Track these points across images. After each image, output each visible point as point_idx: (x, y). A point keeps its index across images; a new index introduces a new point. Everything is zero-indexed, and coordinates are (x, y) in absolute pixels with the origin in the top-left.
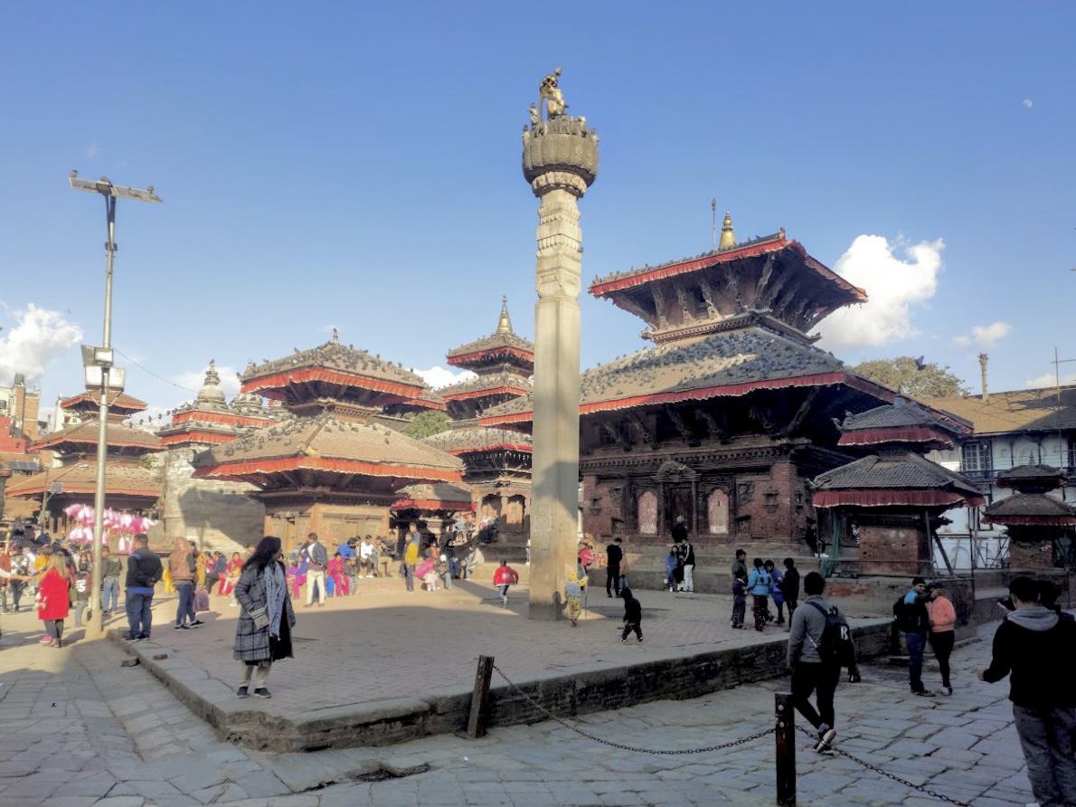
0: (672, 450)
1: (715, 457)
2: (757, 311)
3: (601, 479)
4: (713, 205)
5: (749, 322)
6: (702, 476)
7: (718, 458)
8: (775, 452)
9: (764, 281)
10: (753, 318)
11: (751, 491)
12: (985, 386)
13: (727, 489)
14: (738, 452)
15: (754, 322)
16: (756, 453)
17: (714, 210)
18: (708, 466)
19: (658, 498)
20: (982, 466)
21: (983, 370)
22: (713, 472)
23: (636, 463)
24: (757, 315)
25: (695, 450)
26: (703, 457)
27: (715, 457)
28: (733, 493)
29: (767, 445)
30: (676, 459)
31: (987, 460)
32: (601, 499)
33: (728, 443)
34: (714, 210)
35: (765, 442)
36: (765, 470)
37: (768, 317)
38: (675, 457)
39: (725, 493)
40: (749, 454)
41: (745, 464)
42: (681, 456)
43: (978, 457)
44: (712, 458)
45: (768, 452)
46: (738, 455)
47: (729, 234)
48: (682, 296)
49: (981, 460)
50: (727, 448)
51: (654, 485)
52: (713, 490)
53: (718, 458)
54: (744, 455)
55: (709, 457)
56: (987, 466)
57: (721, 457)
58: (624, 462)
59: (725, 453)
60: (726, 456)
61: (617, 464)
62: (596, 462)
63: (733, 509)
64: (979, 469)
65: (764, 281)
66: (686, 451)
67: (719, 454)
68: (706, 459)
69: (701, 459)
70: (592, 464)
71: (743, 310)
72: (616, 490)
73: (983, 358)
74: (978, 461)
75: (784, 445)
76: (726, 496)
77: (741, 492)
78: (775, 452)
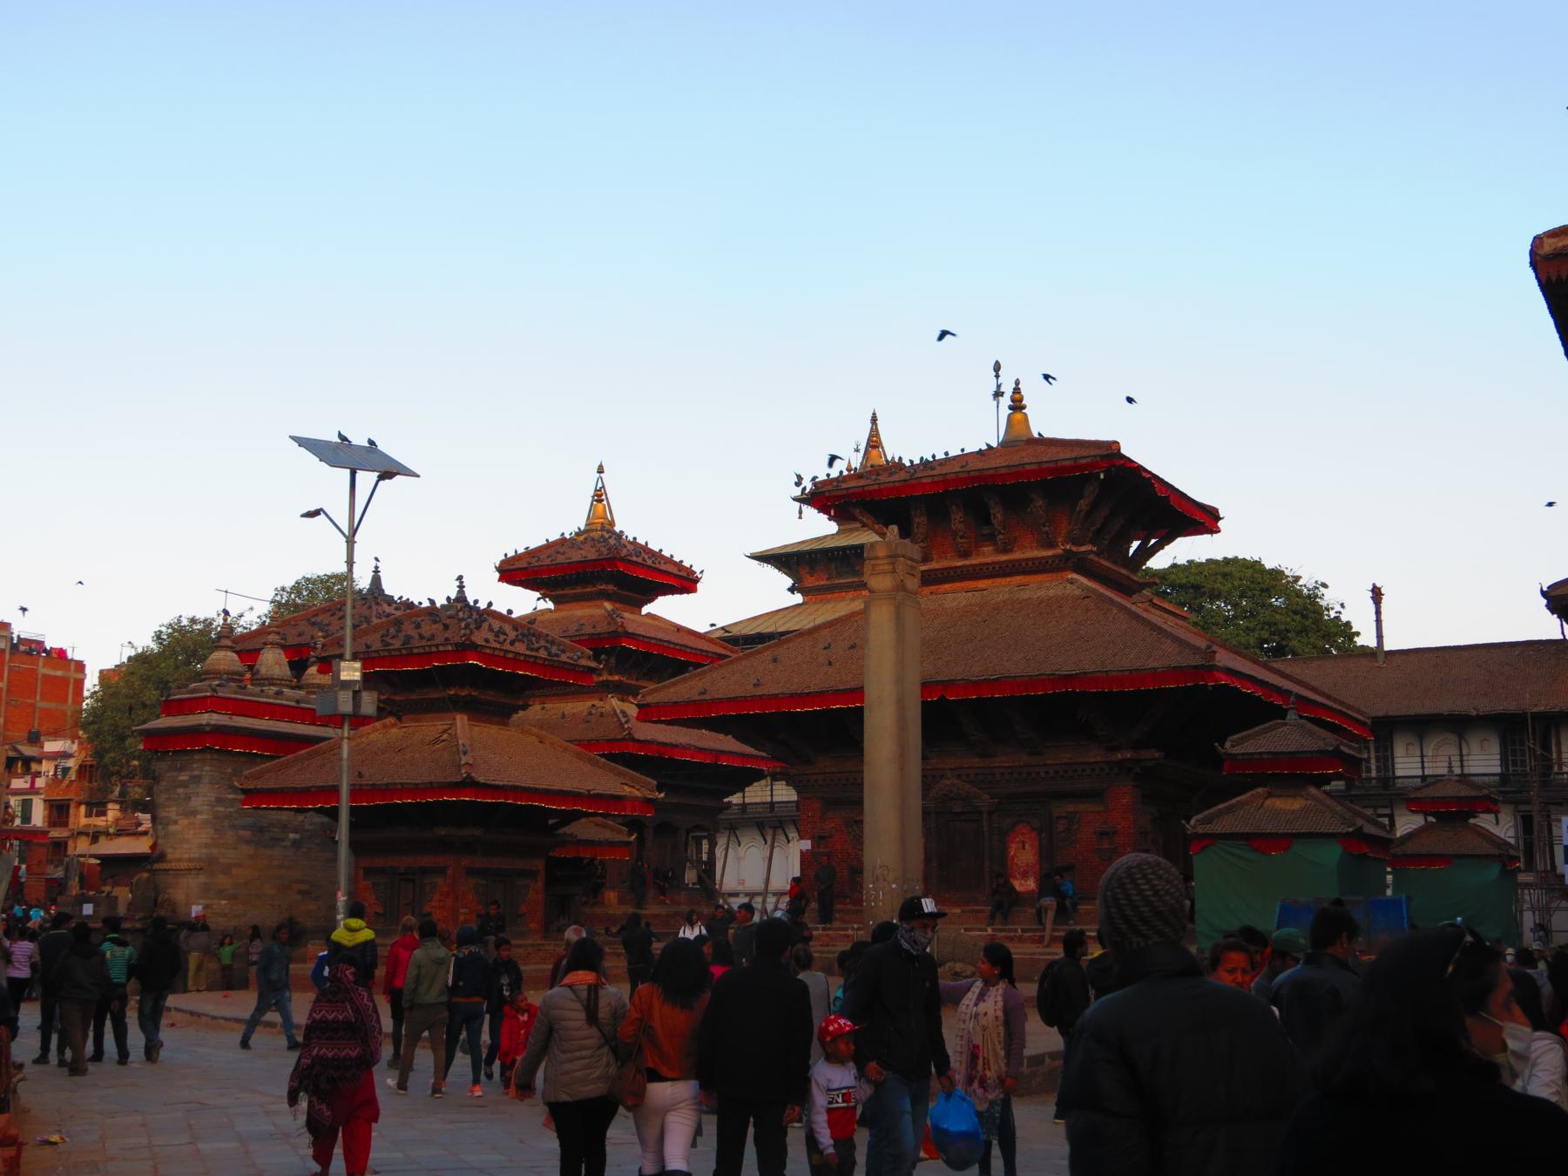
4: (997, 367)
9: (1083, 505)
10: (1068, 559)
12: (1380, 637)
20: (1378, 769)
21: (1378, 613)
24: (1076, 553)
31: (1387, 761)
35: (1095, 755)
37: (1092, 556)
43: (1373, 755)
47: (1018, 416)
48: (957, 519)
49: (1378, 759)
56: (1386, 769)
63: (1046, 853)
64: (1374, 774)
65: (1083, 505)
71: (1051, 545)
73: (1377, 594)
74: (1373, 761)
76: (1034, 834)
77: (1061, 828)
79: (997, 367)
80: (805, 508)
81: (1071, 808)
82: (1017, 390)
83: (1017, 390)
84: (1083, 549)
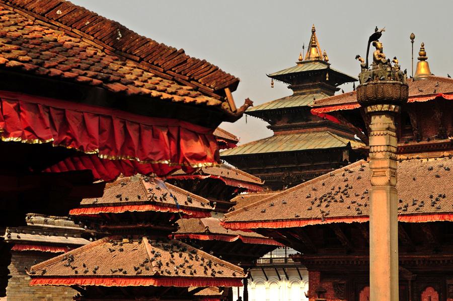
1: (429, 261)
3: (324, 276)
4: (413, 38)
7: (431, 262)
17: (413, 42)
23: (359, 263)
27: (429, 261)
32: (326, 292)
34: (413, 42)
46: (449, 261)
47: (423, 63)
52: (424, 289)
53: (431, 262)
57: (434, 261)
61: (341, 263)
62: (322, 260)
68: (422, 263)
69: (417, 263)
70: (318, 262)
72: (339, 284)
79: (413, 38)
80: (275, 81)
82: (422, 49)
83: (422, 49)
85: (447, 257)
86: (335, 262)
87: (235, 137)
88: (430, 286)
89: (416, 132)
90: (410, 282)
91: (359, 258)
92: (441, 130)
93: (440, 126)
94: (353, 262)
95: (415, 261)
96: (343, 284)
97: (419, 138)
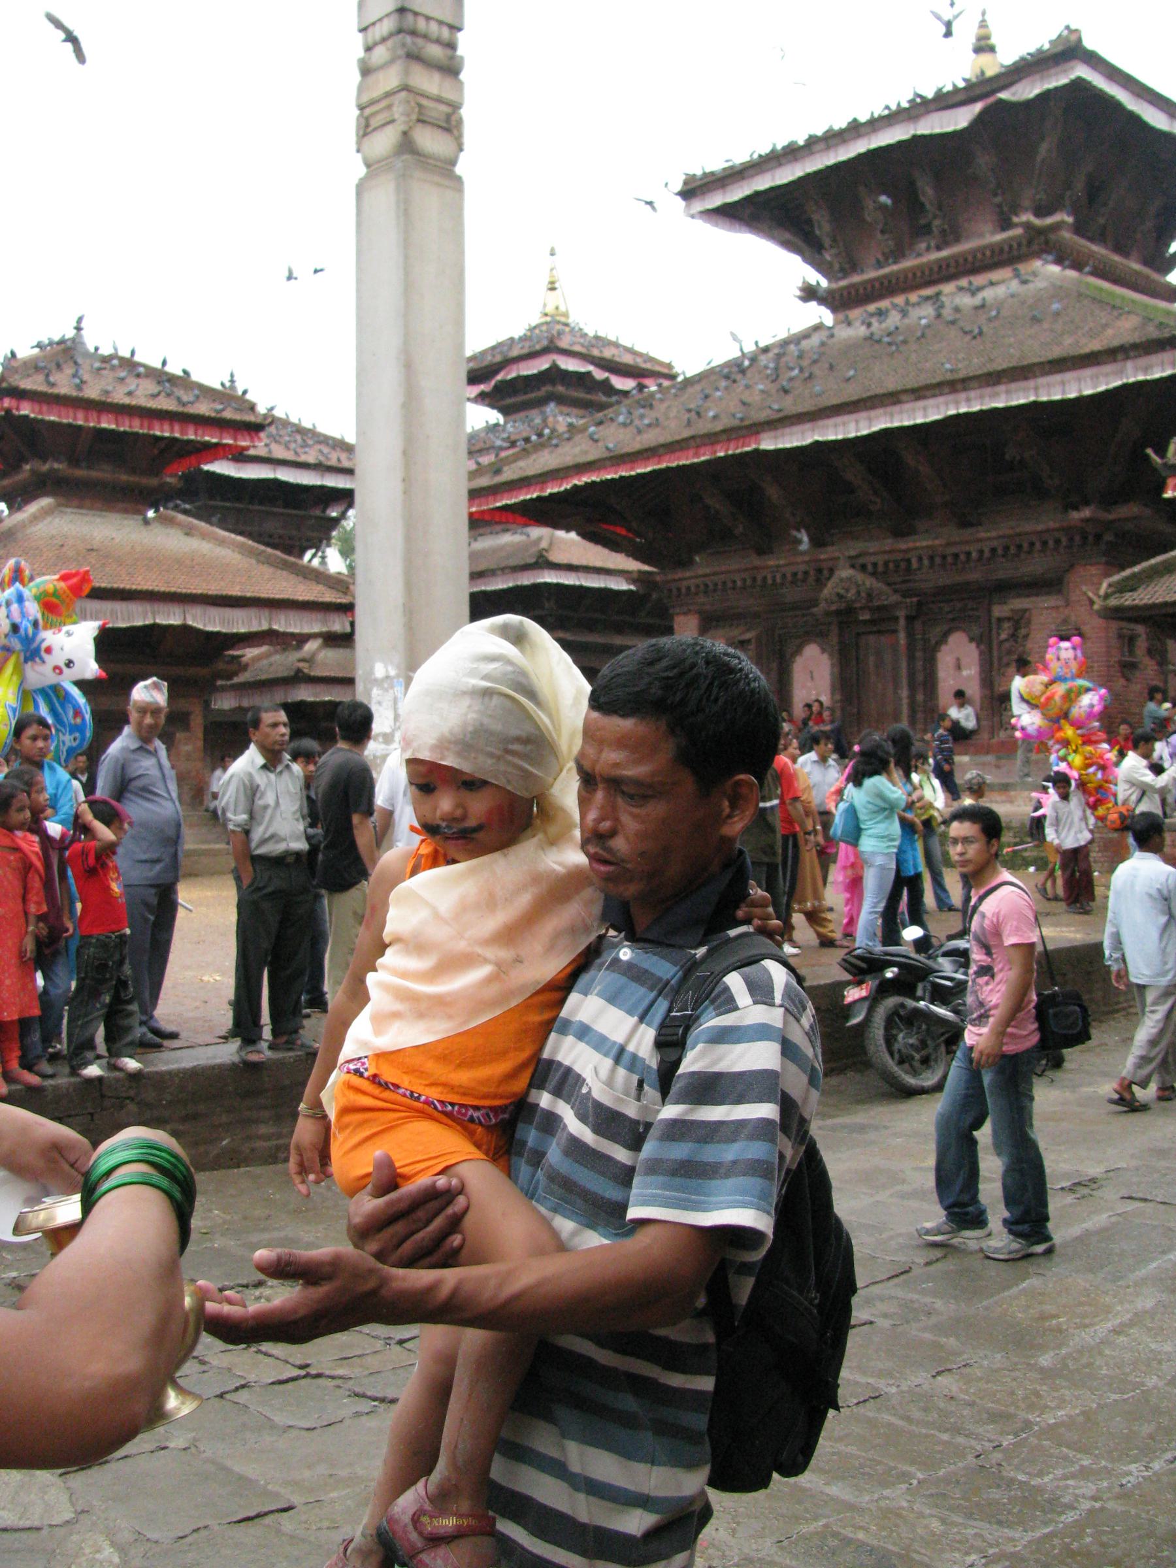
0: (854, 548)
1: (944, 557)
2: (1037, 222)
5: (1024, 249)
6: (920, 604)
7: (950, 559)
8: (1071, 539)
11: (1023, 632)
13: (976, 630)
14: (995, 543)
15: (1035, 247)
16: (1032, 544)
18: (930, 579)
19: (831, 656)
22: (943, 593)
23: (779, 580)
25: (903, 545)
26: (920, 559)
27: (944, 557)
28: (983, 640)
29: (1052, 525)
30: (863, 567)
33: (972, 525)
36: (1050, 584)
38: (861, 561)
39: (971, 640)
40: (1015, 549)
41: (1004, 571)
42: (873, 559)
44: (938, 560)
45: (1058, 542)
46: (993, 550)
50: (968, 533)
51: (815, 633)
52: (945, 636)
53: (950, 559)
54: (1006, 548)
55: (931, 558)
57: (956, 556)
58: (754, 579)
59: (967, 548)
60: (968, 554)
61: (739, 583)
62: (698, 581)
66: (879, 547)
67: (954, 550)
69: (915, 564)
71: (1006, 224)
75: (1087, 520)
77: (1003, 636)
78: (1071, 539)
81: (1018, 603)
82: (983, 24)
83: (983, 24)
84: (1049, 221)
85: (989, 539)
86: (724, 583)
87: (669, 366)
88: (957, 629)
89: (937, 222)
90: (902, 622)
91: (778, 566)
92: (999, 206)
93: (995, 195)
94: (765, 578)
95: (909, 561)
96: (749, 641)
97: (951, 235)
